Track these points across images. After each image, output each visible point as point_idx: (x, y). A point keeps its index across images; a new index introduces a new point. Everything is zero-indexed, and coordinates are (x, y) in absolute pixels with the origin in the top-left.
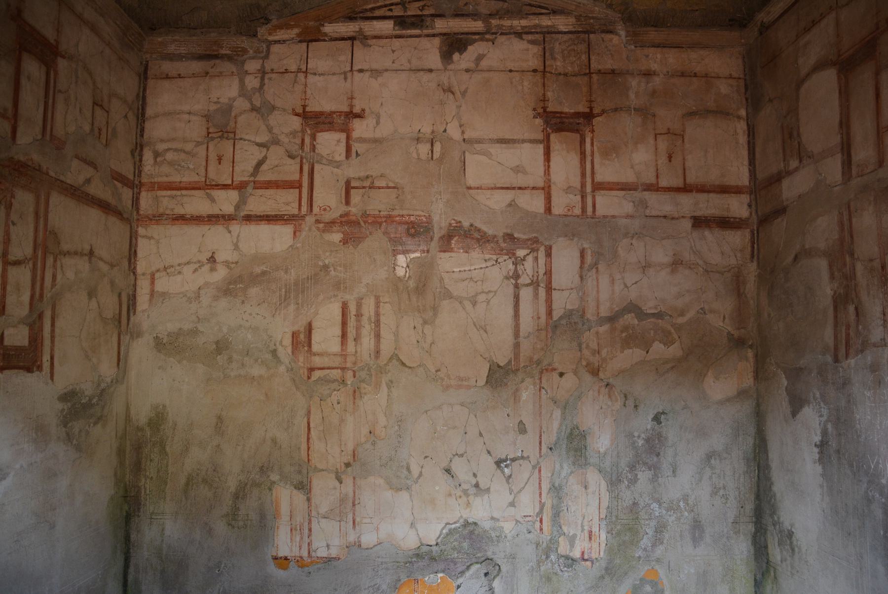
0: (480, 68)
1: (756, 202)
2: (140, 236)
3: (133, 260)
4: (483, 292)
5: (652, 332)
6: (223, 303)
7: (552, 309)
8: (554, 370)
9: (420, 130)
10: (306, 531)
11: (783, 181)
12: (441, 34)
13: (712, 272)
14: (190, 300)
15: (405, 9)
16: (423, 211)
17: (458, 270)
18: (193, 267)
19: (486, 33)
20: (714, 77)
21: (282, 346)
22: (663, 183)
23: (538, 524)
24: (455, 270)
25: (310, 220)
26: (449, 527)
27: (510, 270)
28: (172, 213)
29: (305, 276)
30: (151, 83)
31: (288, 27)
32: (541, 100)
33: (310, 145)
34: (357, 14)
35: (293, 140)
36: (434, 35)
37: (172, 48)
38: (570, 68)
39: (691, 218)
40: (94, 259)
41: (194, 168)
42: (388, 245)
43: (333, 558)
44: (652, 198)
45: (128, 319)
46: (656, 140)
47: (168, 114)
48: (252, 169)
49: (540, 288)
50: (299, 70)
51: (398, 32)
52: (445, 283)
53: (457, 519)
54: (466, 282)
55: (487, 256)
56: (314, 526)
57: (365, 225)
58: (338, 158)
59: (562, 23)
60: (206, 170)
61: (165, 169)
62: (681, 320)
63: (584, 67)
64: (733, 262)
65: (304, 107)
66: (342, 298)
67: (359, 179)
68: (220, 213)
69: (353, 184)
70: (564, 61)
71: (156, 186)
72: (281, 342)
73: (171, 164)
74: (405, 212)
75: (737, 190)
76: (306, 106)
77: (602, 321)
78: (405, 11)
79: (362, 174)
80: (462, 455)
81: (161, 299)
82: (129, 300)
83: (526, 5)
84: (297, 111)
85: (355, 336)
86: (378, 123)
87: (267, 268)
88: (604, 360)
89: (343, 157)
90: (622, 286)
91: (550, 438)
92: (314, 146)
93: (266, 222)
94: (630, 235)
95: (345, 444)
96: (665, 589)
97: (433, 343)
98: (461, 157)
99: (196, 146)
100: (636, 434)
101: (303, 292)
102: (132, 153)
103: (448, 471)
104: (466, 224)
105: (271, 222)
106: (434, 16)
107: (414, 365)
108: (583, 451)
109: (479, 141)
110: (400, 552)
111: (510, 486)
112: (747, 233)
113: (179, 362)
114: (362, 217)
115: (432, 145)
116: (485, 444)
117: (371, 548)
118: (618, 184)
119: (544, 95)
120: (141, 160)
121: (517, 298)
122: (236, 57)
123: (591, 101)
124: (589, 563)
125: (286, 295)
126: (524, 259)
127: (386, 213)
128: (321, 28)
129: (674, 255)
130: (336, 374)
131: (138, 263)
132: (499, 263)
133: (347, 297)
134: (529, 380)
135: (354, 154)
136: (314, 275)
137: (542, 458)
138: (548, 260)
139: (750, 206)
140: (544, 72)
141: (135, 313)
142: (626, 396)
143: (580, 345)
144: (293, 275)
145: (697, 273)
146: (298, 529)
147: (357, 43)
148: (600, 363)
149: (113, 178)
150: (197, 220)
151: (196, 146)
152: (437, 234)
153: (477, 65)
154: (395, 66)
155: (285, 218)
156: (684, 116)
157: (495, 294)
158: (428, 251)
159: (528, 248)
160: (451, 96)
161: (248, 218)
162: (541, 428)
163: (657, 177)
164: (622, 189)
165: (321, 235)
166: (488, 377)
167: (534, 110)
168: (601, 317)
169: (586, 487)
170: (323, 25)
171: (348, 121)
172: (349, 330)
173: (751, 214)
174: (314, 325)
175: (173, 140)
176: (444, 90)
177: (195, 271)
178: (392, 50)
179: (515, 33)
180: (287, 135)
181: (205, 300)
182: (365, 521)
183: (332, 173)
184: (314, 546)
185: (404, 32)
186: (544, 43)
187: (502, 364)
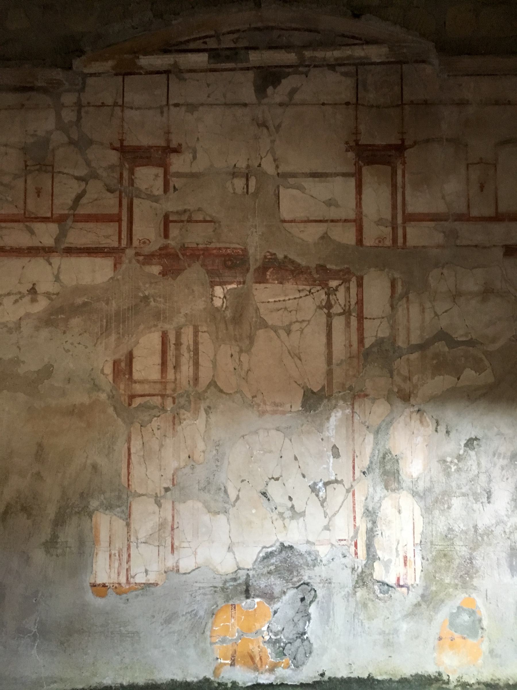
4: (297, 321)
5: (463, 359)
6: (45, 333)
9: (235, 165)
10: (125, 557)
14: (10, 331)
15: (219, 41)
16: (239, 244)
17: (273, 300)
18: (13, 298)
21: (104, 374)
22: (474, 213)
23: (353, 548)
24: (270, 300)
25: (130, 252)
26: (265, 550)
27: (323, 300)
32: (354, 133)
33: (129, 178)
36: (248, 69)
39: (502, 247)
42: (205, 277)
43: (151, 584)
49: (352, 317)
50: (115, 104)
51: (213, 66)
52: (261, 313)
53: (274, 542)
54: (280, 312)
55: (301, 287)
56: (133, 551)
58: (156, 193)
60: (25, 203)
62: (492, 348)
65: (122, 141)
67: (177, 212)
69: (171, 218)
76: (123, 140)
77: (413, 349)
79: (180, 208)
80: (277, 479)
85: (174, 364)
86: (195, 158)
88: (415, 386)
89: (161, 191)
90: (433, 315)
91: (363, 463)
92: (133, 180)
93: (87, 254)
95: (165, 469)
96: (483, 618)
98: (275, 190)
100: (449, 459)
101: (124, 322)
103: (264, 494)
104: (280, 256)
105: (92, 254)
106: (247, 48)
107: (231, 392)
108: (396, 475)
109: (294, 175)
110: (218, 576)
111: (325, 509)
114: (180, 250)
115: (247, 180)
116: (299, 467)
117: (189, 573)
118: (428, 215)
119: (356, 128)
121: (329, 327)
123: (403, 133)
124: (404, 590)
126: (336, 290)
127: (204, 246)
132: (312, 293)
135: (171, 189)
136: (134, 306)
137: (356, 482)
138: (359, 290)
148: (411, 389)
155: (106, 250)
157: (309, 324)
158: (244, 283)
159: (340, 279)
160: (265, 131)
161: (70, 251)
162: (354, 452)
163: (469, 206)
165: (141, 267)
167: (347, 143)
168: (411, 345)
169: (399, 512)
172: (169, 358)
174: (135, 353)
176: (259, 125)
177: (16, 301)
178: (207, 84)
179: (328, 65)
183: (151, 207)
184: (132, 573)
186: (357, 75)
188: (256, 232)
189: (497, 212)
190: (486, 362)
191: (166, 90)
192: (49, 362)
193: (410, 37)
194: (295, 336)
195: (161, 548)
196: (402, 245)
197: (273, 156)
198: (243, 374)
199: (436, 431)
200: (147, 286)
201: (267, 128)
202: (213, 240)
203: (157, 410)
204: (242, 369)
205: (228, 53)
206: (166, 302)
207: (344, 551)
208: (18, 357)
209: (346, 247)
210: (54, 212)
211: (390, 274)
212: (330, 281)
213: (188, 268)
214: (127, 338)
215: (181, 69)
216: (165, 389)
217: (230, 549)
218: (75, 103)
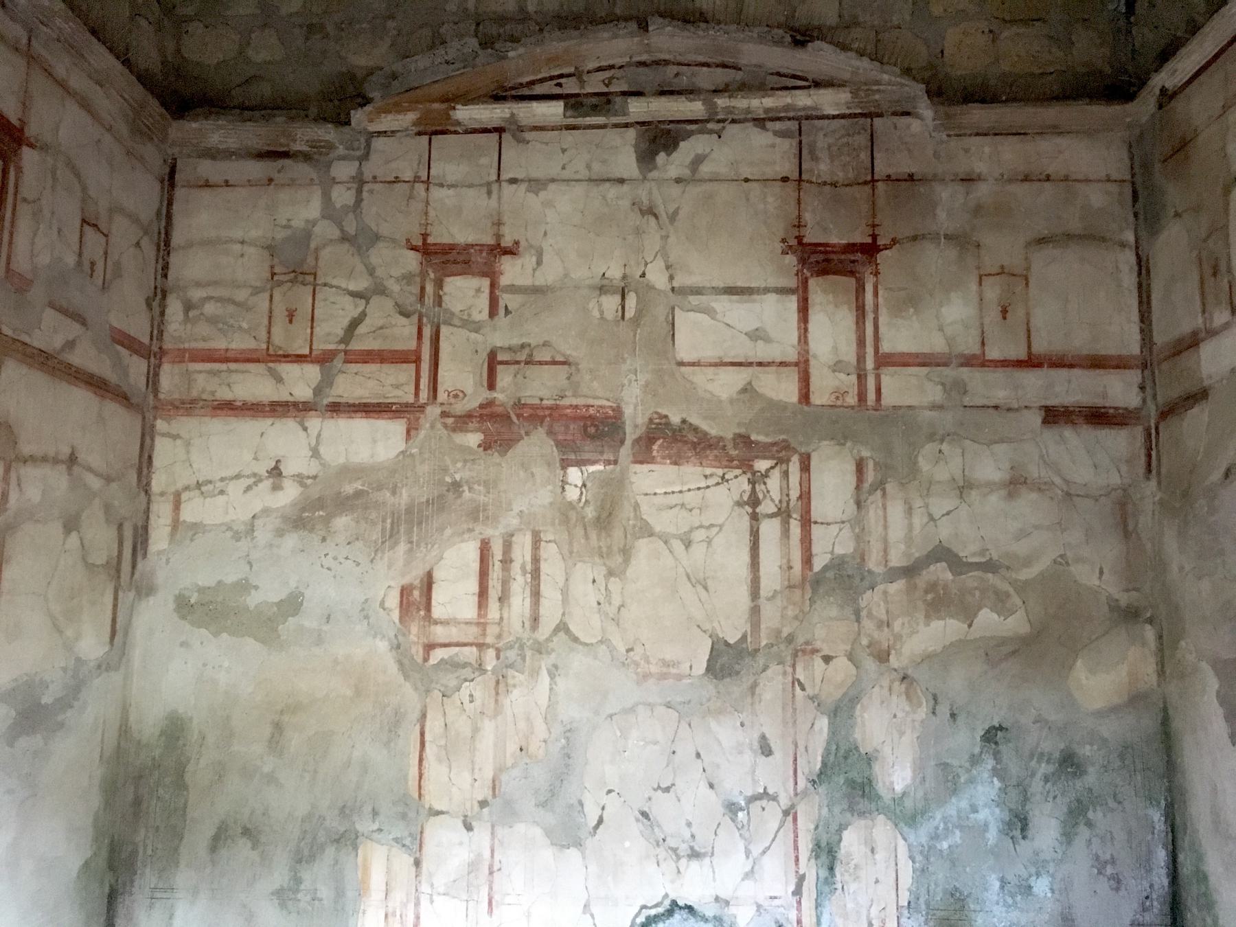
0: (697, 176)
2: (159, 434)
3: (145, 471)
4: (701, 527)
5: (977, 593)
6: (291, 540)
7: (811, 555)
8: (815, 651)
13: (1078, 496)
14: (237, 537)
15: (582, 83)
16: (608, 400)
17: (663, 491)
19: (707, 121)
21: (384, 609)
22: (993, 353)
24: (658, 491)
25: (433, 411)
27: (744, 491)
28: (211, 398)
29: (424, 499)
30: (179, 193)
31: (397, 108)
34: (506, 91)
36: (627, 125)
38: (841, 174)
40: (76, 469)
41: (250, 328)
44: (974, 378)
45: (134, 566)
46: (980, 284)
47: (208, 243)
49: (792, 521)
50: (417, 179)
51: (571, 121)
53: (660, 900)
57: (518, 420)
59: (829, 101)
60: (269, 332)
61: (203, 329)
62: (1026, 574)
64: (1115, 480)
65: (425, 236)
66: (481, 534)
67: (510, 349)
68: (291, 399)
69: (500, 358)
71: (187, 355)
73: (213, 320)
74: (579, 401)
75: (1119, 364)
77: (894, 574)
78: (582, 87)
79: (516, 341)
80: (667, 790)
81: (190, 533)
82: (135, 537)
83: (772, 74)
84: (414, 243)
87: (363, 485)
88: (898, 637)
89: (485, 315)
90: (925, 519)
92: (440, 297)
97: (623, 606)
98: (668, 316)
99: (252, 295)
101: (420, 523)
104: (675, 419)
105: (371, 414)
107: (594, 641)
109: (698, 291)
112: (1139, 431)
118: (917, 355)
119: (799, 217)
120: (162, 314)
121: (755, 535)
123: (874, 226)
125: (392, 528)
126: (766, 475)
127: (551, 402)
128: (451, 113)
129: (1012, 468)
130: (470, 653)
131: (154, 476)
132: (727, 481)
133: (489, 532)
134: (774, 669)
135: (502, 311)
138: (804, 476)
139: (1142, 388)
140: (800, 180)
141: (145, 555)
142: (935, 698)
143: (857, 613)
144: (404, 497)
145: (1052, 498)
146: (398, 914)
147: (506, 137)
148: (891, 642)
151: (252, 295)
152: (631, 434)
154: (566, 174)
155: (394, 408)
156: (1028, 245)
157: (721, 530)
158: (616, 462)
159: (772, 458)
160: (652, 220)
161: (336, 409)
163: (983, 344)
164: (924, 365)
166: (709, 661)
167: (783, 241)
168: (891, 568)
169: (873, 851)
170: (454, 108)
171: (493, 259)
172: (491, 583)
173: (1144, 401)
174: (437, 575)
175: (216, 283)
177: (249, 488)
179: (755, 120)
181: (263, 534)
182: (508, 900)
186: (800, 135)
187: (732, 642)
189: (1030, 354)
190: (1016, 600)
191: (496, 158)
192: (297, 588)
193: (886, 77)
194: (698, 551)
195: (471, 904)
196: (874, 404)
197: (665, 261)
198: (612, 611)
199: (934, 713)
200: (459, 465)
203: (469, 669)
204: (610, 604)
205: (594, 100)
206: (489, 493)
207: (779, 917)
208: (246, 579)
209: (782, 406)
210: (314, 347)
211: (855, 451)
216: (484, 635)
217: (586, 907)
218: (353, 177)
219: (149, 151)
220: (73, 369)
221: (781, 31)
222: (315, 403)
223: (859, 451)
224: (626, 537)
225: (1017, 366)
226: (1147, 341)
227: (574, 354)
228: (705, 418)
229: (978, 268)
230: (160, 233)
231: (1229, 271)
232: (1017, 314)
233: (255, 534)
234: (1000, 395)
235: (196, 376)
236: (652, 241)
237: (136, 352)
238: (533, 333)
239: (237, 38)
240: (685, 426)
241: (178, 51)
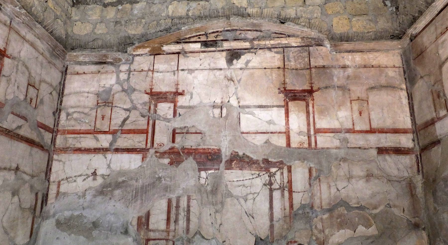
0: (248, 67)
1: (418, 138)
3: (48, 174)
4: (251, 193)
5: (357, 219)
11: (436, 123)
12: (226, 50)
14: (79, 197)
15: (207, 37)
16: (216, 146)
19: (252, 48)
20: (385, 67)
22: (357, 128)
25: (152, 151)
30: (68, 76)
31: (144, 47)
34: (181, 40)
35: (145, 107)
36: (223, 51)
37: (81, 59)
38: (299, 66)
40: (19, 173)
41: (88, 122)
45: (42, 208)
46: (351, 104)
47: (77, 93)
48: (121, 123)
49: (285, 191)
50: (149, 70)
51: (203, 49)
54: (241, 188)
59: (293, 42)
60: (95, 123)
61: (72, 122)
63: (307, 65)
64: (406, 174)
65: (151, 89)
67: (180, 128)
68: (101, 147)
69: (177, 131)
70: (295, 62)
72: (131, 223)
74: (206, 147)
75: (405, 132)
76: (152, 89)
78: (207, 38)
79: (182, 126)
81: (62, 197)
82: (43, 197)
86: (191, 98)
87: (125, 178)
90: (336, 190)
92: (156, 110)
94: (339, 159)
97: (221, 224)
98: (238, 116)
99: (90, 110)
101: (146, 193)
102: (54, 114)
104: (241, 154)
105: (130, 152)
109: (248, 107)
112: (413, 156)
113: (69, 235)
115: (221, 110)
118: (329, 129)
119: (284, 81)
120: (59, 118)
122: (115, 63)
126: (275, 174)
129: (367, 171)
131: (51, 175)
132: (260, 176)
135: (178, 115)
138: (289, 174)
139: (413, 140)
140: (284, 68)
141: (46, 205)
144: (140, 183)
149: (39, 126)
150: (88, 151)
151: (90, 110)
153: (246, 66)
154: (201, 67)
155: (138, 150)
156: (367, 89)
158: (219, 169)
159: (277, 167)
160: (232, 83)
161: (117, 150)
163: (353, 124)
164: (332, 132)
167: (279, 89)
170: (163, 46)
172: (171, 215)
173: (415, 145)
174: (151, 212)
176: (228, 80)
177: (84, 180)
179: (267, 48)
180: (141, 104)
181: (88, 197)
183: (165, 125)
185: (206, 49)
186: (284, 53)
187: (263, 238)
188: (226, 139)
189: (371, 128)
191: (177, 63)
194: (250, 203)
198: (217, 226)
201: (233, 81)
202: (201, 144)
206: (171, 181)
209: (281, 148)
211: (308, 165)
212: (271, 168)
213: (186, 160)
214: (147, 203)
215: (185, 52)
216: (169, 235)
218: (127, 70)
219: (58, 63)
220: (20, 136)
221: (276, 20)
222: (110, 148)
223: (310, 165)
224: (222, 198)
225: (365, 133)
226: (414, 123)
227: (204, 130)
228: (252, 153)
229: (350, 98)
230: (60, 90)
231: (444, 95)
232: (365, 115)
233: (86, 196)
234: (361, 143)
235: (69, 139)
236: (232, 89)
237: (48, 131)
238: (189, 122)
239: (92, 26)
240: (244, 156)
241: (72, 31)
